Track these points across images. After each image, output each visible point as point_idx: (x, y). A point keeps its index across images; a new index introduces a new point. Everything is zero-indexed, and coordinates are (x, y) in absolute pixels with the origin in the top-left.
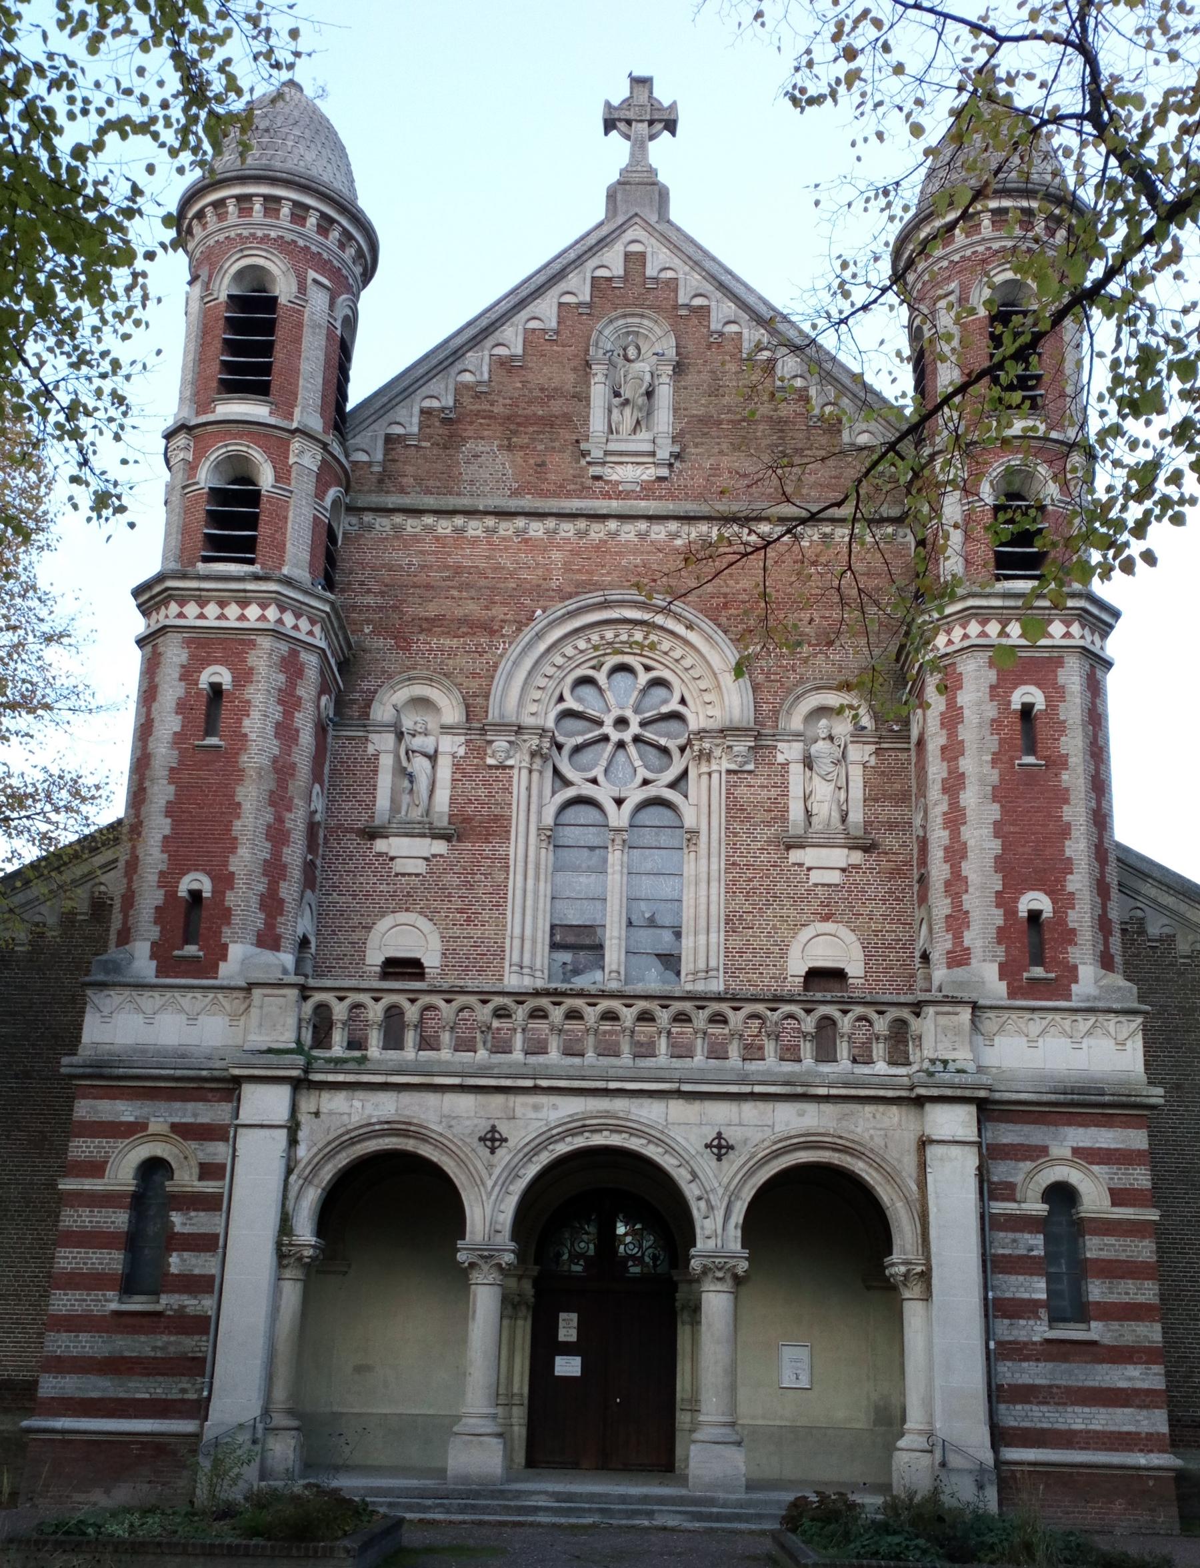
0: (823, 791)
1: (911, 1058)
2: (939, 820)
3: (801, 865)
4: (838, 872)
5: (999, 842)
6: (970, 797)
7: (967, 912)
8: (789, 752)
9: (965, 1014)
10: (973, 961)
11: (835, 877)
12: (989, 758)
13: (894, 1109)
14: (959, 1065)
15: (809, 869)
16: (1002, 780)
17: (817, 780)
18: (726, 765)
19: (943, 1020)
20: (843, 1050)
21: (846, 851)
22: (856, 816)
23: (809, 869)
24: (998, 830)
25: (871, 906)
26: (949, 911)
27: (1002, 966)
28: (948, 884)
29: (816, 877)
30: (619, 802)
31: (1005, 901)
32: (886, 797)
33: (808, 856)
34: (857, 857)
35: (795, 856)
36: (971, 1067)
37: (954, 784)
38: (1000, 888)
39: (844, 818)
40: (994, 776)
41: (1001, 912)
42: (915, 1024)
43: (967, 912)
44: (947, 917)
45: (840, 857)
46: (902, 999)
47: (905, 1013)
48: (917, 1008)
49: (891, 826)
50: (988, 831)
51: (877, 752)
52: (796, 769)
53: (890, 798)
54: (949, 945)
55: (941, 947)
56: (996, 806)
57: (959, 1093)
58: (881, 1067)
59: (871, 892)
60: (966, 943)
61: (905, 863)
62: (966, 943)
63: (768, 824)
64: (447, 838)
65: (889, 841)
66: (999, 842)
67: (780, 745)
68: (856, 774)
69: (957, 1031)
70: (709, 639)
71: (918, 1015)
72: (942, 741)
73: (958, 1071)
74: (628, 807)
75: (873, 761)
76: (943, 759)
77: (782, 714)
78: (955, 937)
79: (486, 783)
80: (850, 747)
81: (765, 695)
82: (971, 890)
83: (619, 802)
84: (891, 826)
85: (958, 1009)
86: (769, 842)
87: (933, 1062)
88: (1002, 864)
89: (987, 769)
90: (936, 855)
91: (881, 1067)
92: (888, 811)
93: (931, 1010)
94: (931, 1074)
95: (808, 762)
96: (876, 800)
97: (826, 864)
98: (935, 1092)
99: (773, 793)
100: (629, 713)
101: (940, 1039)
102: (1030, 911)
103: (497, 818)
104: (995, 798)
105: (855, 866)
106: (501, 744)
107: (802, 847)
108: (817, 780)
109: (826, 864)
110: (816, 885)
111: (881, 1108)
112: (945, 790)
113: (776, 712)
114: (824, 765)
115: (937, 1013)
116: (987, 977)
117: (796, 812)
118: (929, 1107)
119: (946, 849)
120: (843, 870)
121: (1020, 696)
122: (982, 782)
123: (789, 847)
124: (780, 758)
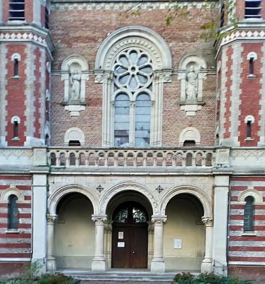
0: (191, 88)
1: (212, 164)
2: (224, 95)
3: (184, 110)
4: (194, 112)
5: (241, 101)
6: (233, 88)
7: (230, 122)
8: (181, 76)
9: (228, 151)
10: (231, 136)
11: (193, 114)
12: (239, 75)
13: (207, 178)
14: (225, 165)
15: (186, 111)
16: (243, 82)
17: (189, 84)
19: (222, 153)
21: (197, 106)
22: (200, 95)
23: (186, 111)
24: (241, 97)
25: (203, 121)
26: (225, 122)
27: (239, 137)
28: (225, 114)
29: (188, 114)
31: (241, 118)
34: (200, 107)
35: (182, 108)
36: (228, 166)
37: (229, 84)
38: (240, 114)
39: (196, 96)
40: (241, 81)
41: (240, 121)
42: (214, 155)
43: (230, 122)
44: (225, 123)
45: (195, 107)
46: (211, 147)
47: (211, 151)
48: (215, 150)
49: (210, 98)
50: (238, 97)
51: (207, 75)
52: (183, 81)
53: (210, 89)
54: (224, 132)
55: (222, 132)
56: (241, 90)
57: (225, 173)
58: (204, 167)
59: (203, 118)
60: (230, 131)
61: (213, 109)
62: (230, 131)
63: (175, 98)
65: (209, 102)
66: (241, 101)
67: (179, 74)
68: (201, 83)
69: (225, 156)
71: (215, 152)
72: (226, 70)
73: (225, 167)
75: (206, 78)
76: (226, 76)
77: (180, 65)
78: (227, 129)
80: (199, 74)
81: (175, 58)
82: (232, 115)
84: (210, 98)
85: (226, 150)
86: (175, 104)
87: (218, 165)
88: (241, 108)
89: (239, 78)
90: (223, 105)
91: (204, 167)
93: (218, 150)
94: (217, 168)
95: (187, 79)
96: (206, 90)
97: (191, 110)
98: (218, 173)
99: (177, 89)
101: (220, 158)
102: (248, 121)
104: (241, 87)
105: (200, 110)
107: (184, 105)
108: (189, 84)
109: (191, 110)
110: (188, 116)
111: (203, 178)
112: (226, 86)
113: (178, 64)
114: (191, 80)
115: (220, 151)
116: (235, 141)
117: (183, 95)
118: (216, 177)
119: (226, 103)
120: (196, 111)
121: (249, 57)
122: (237, 82)
123: (181, 105)
124: (179, 78)
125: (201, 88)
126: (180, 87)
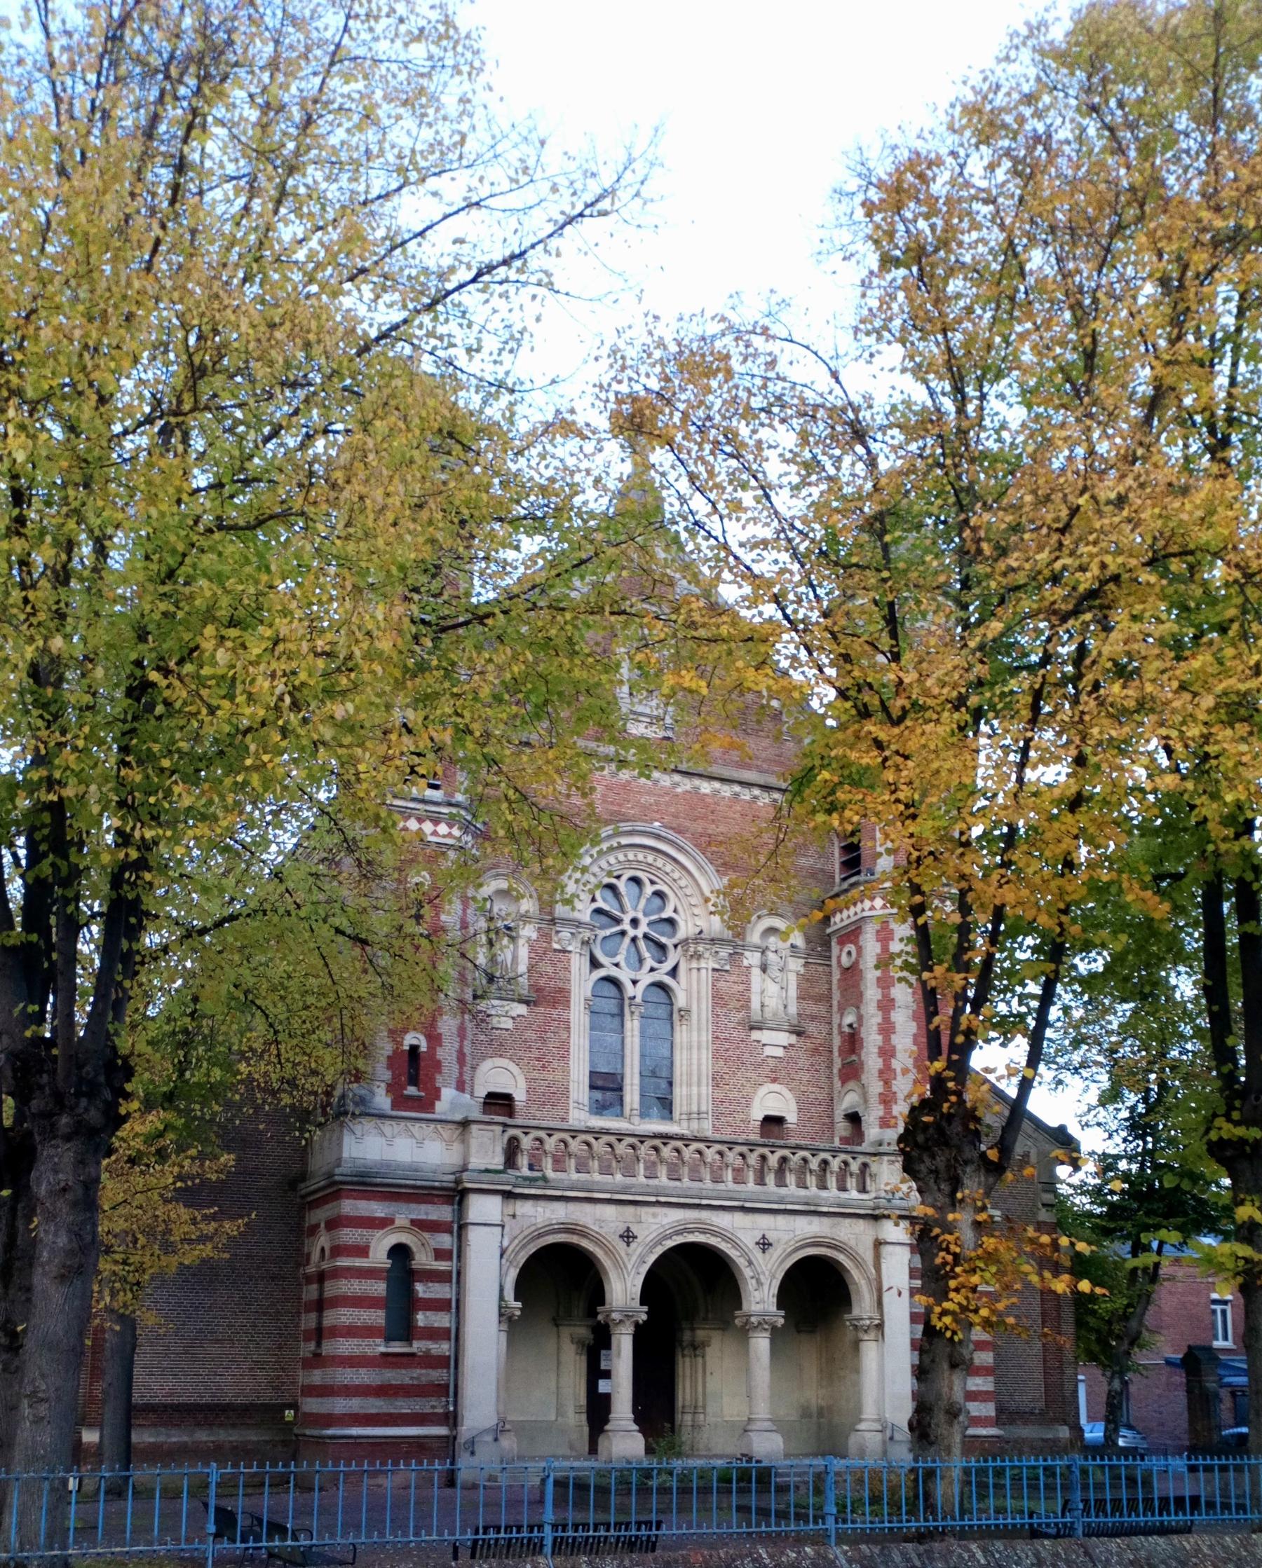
11: (780, 1052)
18: (712, 964)
20: (832, 1181)
22: (793, 1009)
28: (881, 1072)
29: (769, 1051)
30: (634, 982)
32: (811, 997)
33: (764, 1036)
34: (793, 1039)
35: (756, 1035)
42: (874, 1167)
45: (785, 1038)
52: (756, 972)
64: (527, 1003)
65: (812, 1028)
70: (700, 868)
74: (641, 986)
79: (553, 963)
83: (634, 982)
92: (812, 1008)
95: (764, 968)
97: (775, 1042)
100: (640, 916)
103: (561, 990)
106: (565, 934)
114: (774, 971)
117: (755, 1004)
125: (793, 992)
126: (747, 983)
